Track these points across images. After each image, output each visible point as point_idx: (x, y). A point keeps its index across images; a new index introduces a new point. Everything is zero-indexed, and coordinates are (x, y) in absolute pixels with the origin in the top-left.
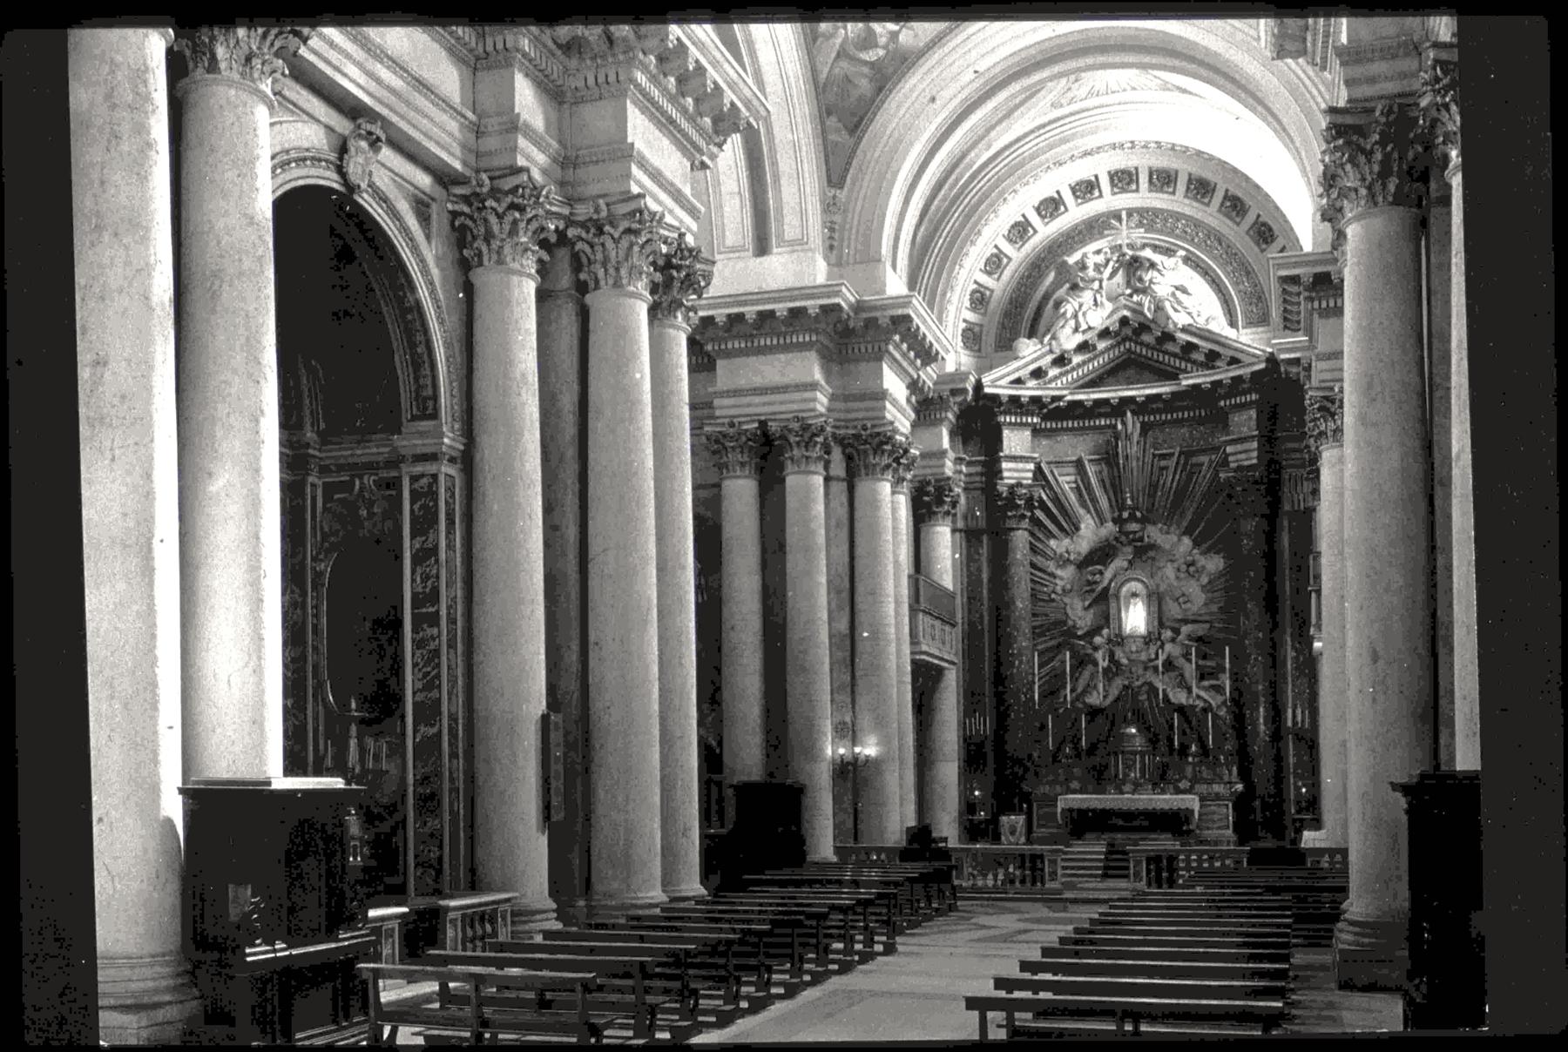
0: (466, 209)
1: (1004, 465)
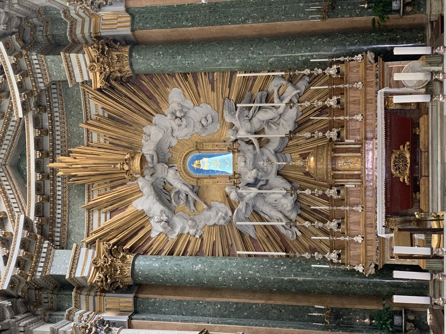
1: (78, 274)
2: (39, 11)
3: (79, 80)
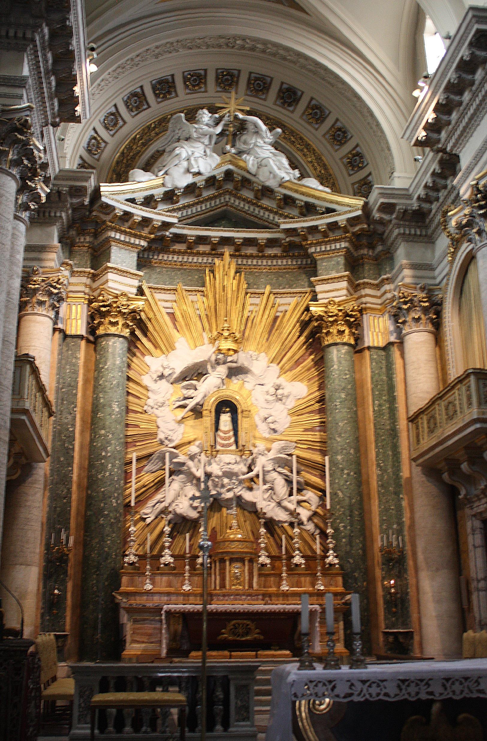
2: (389, 252)
3: (318, 288)
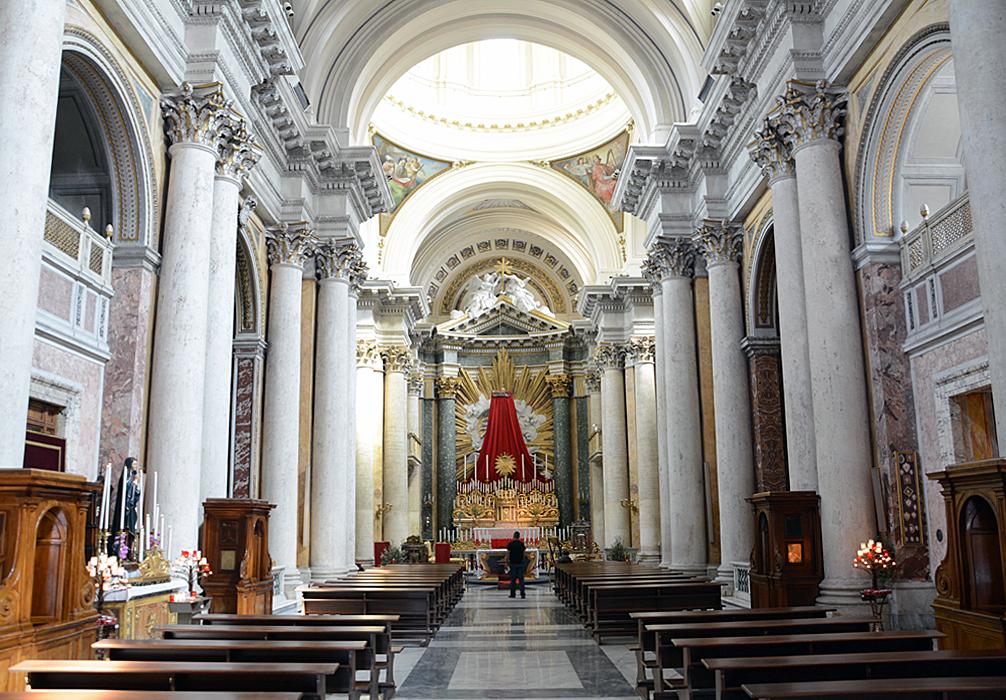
0: (274, 237)
1: (445, 368)
